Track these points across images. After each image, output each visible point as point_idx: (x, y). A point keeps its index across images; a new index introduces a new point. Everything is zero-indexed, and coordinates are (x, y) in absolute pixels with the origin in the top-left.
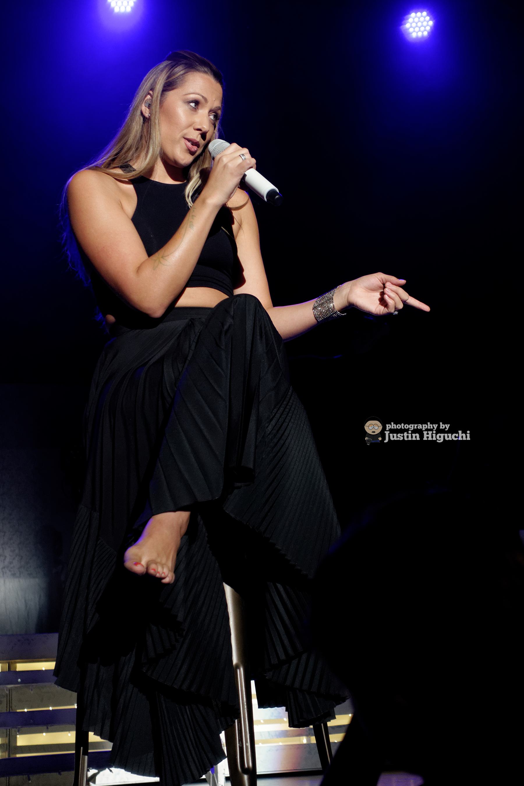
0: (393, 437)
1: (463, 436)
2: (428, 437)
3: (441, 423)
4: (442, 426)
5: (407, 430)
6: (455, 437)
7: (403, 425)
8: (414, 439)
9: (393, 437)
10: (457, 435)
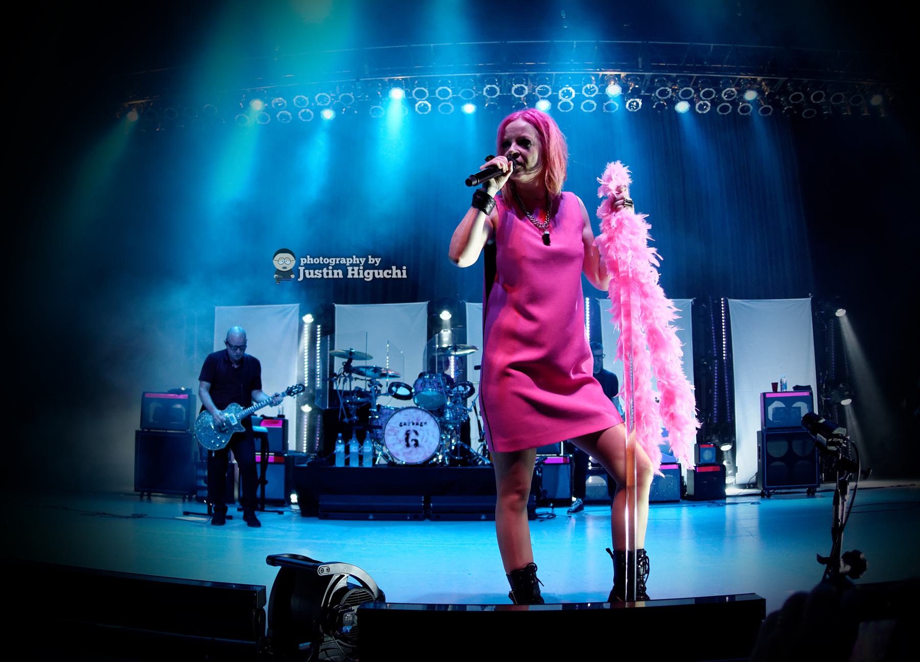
2: (353, 275)
6: (388, 274)
10: (390, 272)
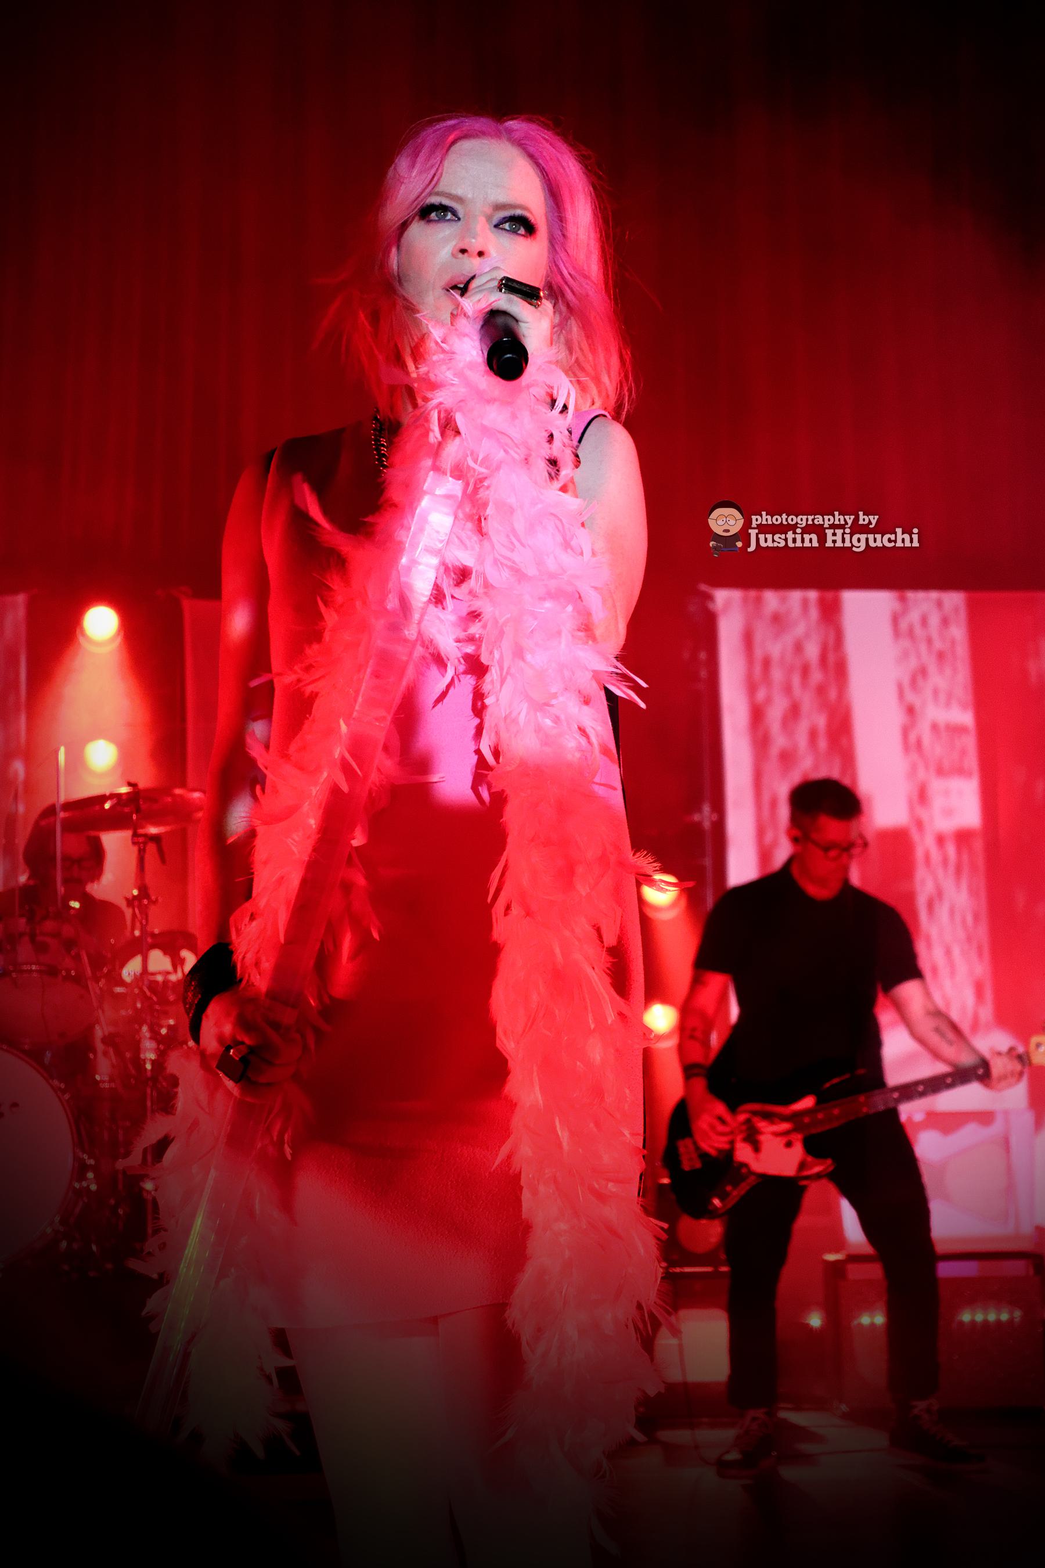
0: (766, 540)
1: (904, 539)
2: (834, 542)
3: (861, 513)
4: (863, 519)
5: (793, 528)
6: (890, 541)
7: (784, 516)
8: (807, 544)
9: (766, 540)
10: (893, 537)
